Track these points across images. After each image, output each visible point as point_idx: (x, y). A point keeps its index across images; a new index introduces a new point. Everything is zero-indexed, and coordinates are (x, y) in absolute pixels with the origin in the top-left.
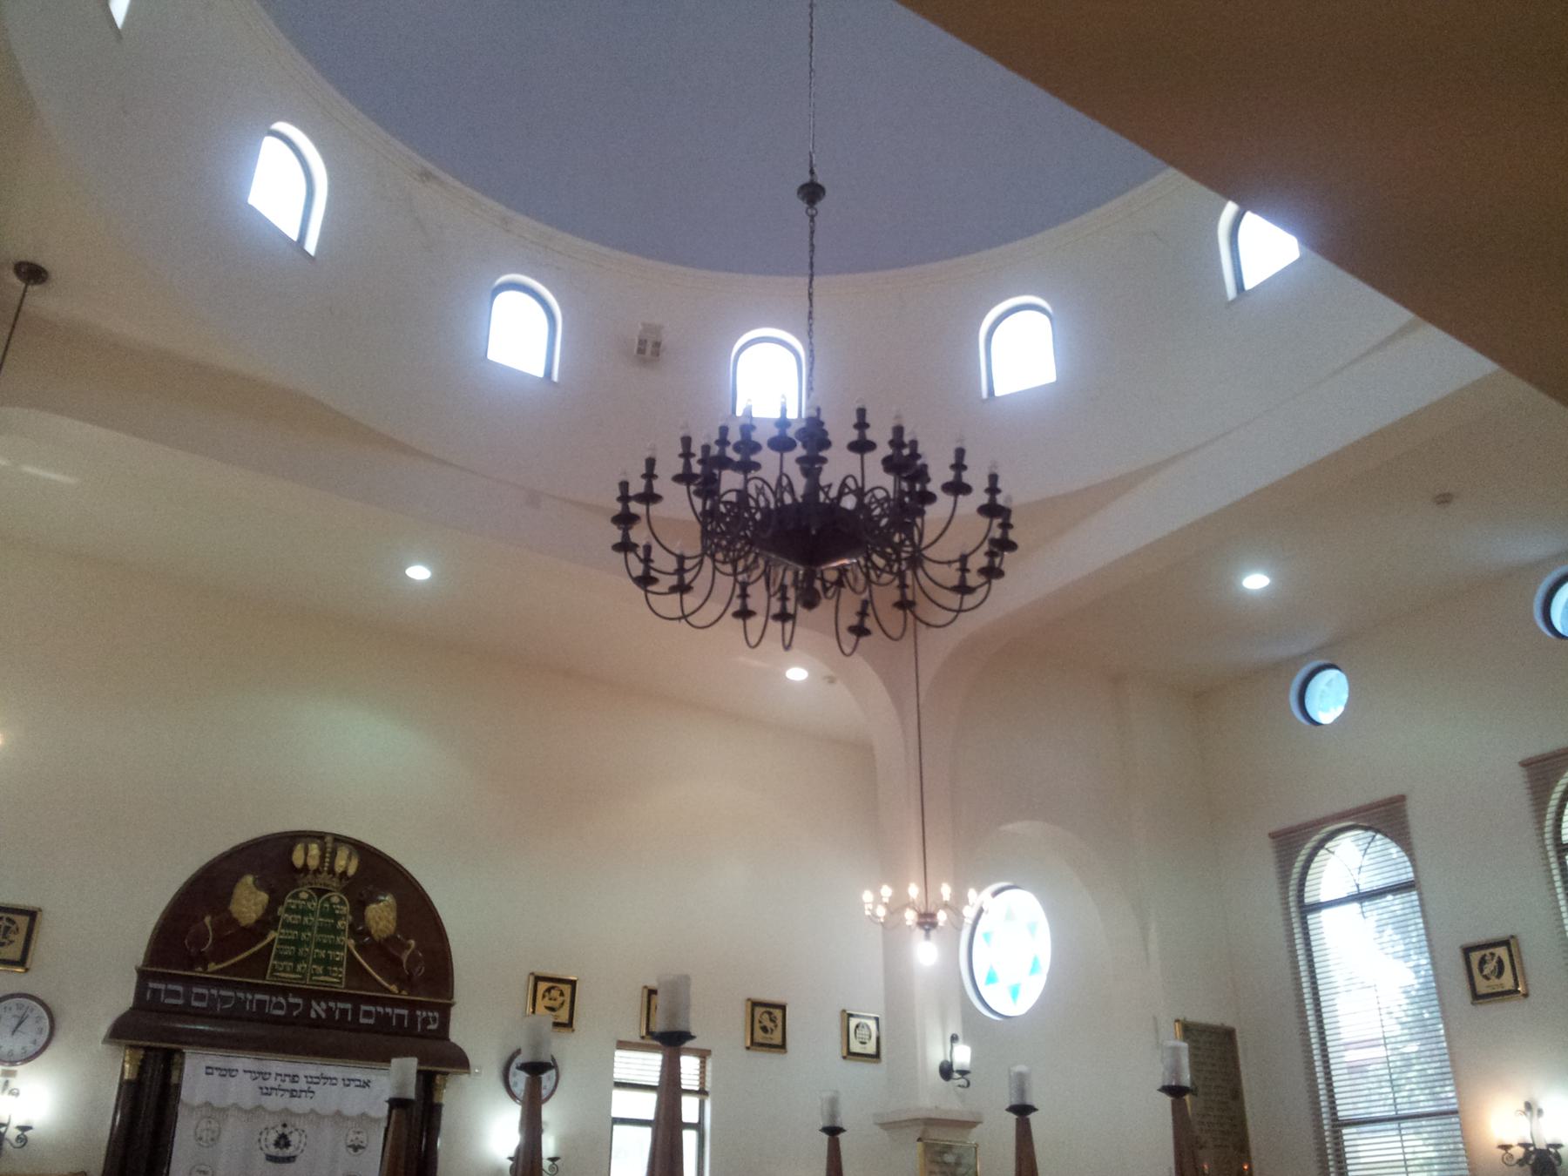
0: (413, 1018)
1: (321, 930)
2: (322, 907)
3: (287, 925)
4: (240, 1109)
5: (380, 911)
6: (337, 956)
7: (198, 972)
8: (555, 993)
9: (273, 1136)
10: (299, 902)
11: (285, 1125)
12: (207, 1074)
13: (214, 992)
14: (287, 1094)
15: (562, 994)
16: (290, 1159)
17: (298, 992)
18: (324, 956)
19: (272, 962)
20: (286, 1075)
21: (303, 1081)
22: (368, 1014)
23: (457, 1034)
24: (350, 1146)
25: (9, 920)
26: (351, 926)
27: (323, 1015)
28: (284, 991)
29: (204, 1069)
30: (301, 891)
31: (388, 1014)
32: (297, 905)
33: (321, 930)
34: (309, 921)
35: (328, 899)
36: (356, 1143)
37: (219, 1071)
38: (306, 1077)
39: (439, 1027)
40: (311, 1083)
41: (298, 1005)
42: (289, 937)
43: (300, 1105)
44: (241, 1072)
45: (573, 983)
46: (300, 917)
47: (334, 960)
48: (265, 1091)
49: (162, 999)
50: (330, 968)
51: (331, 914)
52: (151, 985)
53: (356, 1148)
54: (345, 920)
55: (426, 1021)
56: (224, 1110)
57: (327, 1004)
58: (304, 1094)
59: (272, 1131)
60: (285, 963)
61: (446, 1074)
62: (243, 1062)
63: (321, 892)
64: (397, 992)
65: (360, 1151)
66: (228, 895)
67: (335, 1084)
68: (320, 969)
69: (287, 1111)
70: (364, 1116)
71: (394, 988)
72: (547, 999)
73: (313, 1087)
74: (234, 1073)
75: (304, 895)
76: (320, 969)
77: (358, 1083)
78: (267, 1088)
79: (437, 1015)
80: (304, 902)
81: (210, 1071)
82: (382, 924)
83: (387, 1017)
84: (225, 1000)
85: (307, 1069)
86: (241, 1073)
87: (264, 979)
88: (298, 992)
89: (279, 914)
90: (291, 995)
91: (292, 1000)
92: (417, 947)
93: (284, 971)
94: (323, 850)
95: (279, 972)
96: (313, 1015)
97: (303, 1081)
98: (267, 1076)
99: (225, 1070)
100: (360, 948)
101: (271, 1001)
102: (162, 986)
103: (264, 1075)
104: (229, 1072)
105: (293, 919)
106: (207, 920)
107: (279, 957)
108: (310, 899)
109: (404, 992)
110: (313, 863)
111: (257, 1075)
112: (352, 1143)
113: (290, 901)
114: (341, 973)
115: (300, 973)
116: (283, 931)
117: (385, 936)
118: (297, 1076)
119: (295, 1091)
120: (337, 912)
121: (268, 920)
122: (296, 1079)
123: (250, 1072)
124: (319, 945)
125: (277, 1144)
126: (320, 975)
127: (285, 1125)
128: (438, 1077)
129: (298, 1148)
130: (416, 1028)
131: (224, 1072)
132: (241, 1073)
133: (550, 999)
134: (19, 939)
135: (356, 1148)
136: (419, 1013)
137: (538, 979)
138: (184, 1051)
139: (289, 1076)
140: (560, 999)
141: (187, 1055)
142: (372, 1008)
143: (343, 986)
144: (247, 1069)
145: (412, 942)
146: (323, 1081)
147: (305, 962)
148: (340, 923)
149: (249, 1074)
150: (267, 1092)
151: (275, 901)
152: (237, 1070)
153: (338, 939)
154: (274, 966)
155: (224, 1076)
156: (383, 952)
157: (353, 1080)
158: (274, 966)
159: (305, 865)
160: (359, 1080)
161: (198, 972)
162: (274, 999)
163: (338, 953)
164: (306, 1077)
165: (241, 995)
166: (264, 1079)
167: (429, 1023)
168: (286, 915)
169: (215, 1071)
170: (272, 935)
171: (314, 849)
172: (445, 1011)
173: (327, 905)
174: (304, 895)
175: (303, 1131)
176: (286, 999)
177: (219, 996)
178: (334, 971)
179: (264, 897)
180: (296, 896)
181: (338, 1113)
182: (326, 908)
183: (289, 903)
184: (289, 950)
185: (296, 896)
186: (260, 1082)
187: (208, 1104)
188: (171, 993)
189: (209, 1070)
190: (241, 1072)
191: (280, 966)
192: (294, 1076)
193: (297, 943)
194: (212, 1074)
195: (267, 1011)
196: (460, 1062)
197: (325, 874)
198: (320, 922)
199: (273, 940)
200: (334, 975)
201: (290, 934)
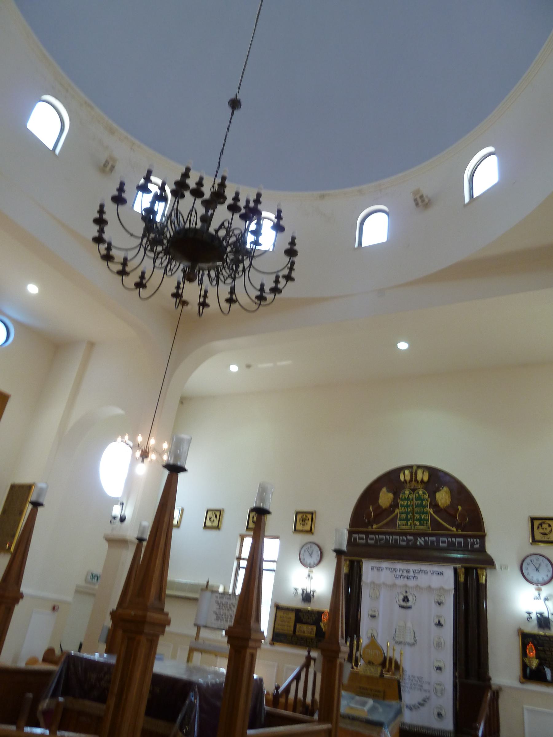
0: (466, 543)
1: (417, 506)
2: (415, 495)
3: (402, 506)
4: (385, 584)
8: (545, 526)
9: (401, 597)
13: (377, 536)
14: (406, 579)
16: (409, 608)
17: (411, 534)
22: (443, 542)
23: (491, 548)
26: (430, 503)
27: (423, 543)
28: (405, 534)
31: (454, 542)
33: (417, 506)
36: (439, 601)
41: (412, 540)
43: (411, 583)
51: (420, 498)
55: (473, 544)
62: (385, 564)
66: (378, 498)
68: (418, 523)
69: (406, 586)
75: (407, 492)
79: (478, 540)
82: (443, 501)
83: (453, 544)
84: (381, 540)
85: (413, 567)
88: (411, 534)
89: (398, 501)
92: (462, 509)
93: (403, 525)
96: (418, 543)
100: (434, 512)
103: (395, 570)
104: (380, 569)
106: (371, 508)
108: (410, 493)
110: (408, 478)
117: (446, 505)
121: (394, 505)
124: (417, 513)
125: (404, 600)
127: (406, 592)
132: (385, 570)
134: (309, 523)
135: (439, 604)
136: (469, 540)
137: (533, 520)
140: (549, 529)
141: (363, 562)
142: (445, 539)
145: (460, 508)
147: (412, 521)
150: (396, 577)
151: (396, 495)
153: (425, 510)
159: (405, 480)
161: (370, 529)
162: (401, 538)
165: (388, 537)
170: (397, 511)
171: (407, 472)
172: (483, 537)
173: (417, 495)
174: (407, 492)
179: (391, 495)
181: (429, 588)
184: (404, 516)
185: (404, 493)
187: (373, 583)
188: (361, 539)
193: (407, 513)
199: (397, 514)
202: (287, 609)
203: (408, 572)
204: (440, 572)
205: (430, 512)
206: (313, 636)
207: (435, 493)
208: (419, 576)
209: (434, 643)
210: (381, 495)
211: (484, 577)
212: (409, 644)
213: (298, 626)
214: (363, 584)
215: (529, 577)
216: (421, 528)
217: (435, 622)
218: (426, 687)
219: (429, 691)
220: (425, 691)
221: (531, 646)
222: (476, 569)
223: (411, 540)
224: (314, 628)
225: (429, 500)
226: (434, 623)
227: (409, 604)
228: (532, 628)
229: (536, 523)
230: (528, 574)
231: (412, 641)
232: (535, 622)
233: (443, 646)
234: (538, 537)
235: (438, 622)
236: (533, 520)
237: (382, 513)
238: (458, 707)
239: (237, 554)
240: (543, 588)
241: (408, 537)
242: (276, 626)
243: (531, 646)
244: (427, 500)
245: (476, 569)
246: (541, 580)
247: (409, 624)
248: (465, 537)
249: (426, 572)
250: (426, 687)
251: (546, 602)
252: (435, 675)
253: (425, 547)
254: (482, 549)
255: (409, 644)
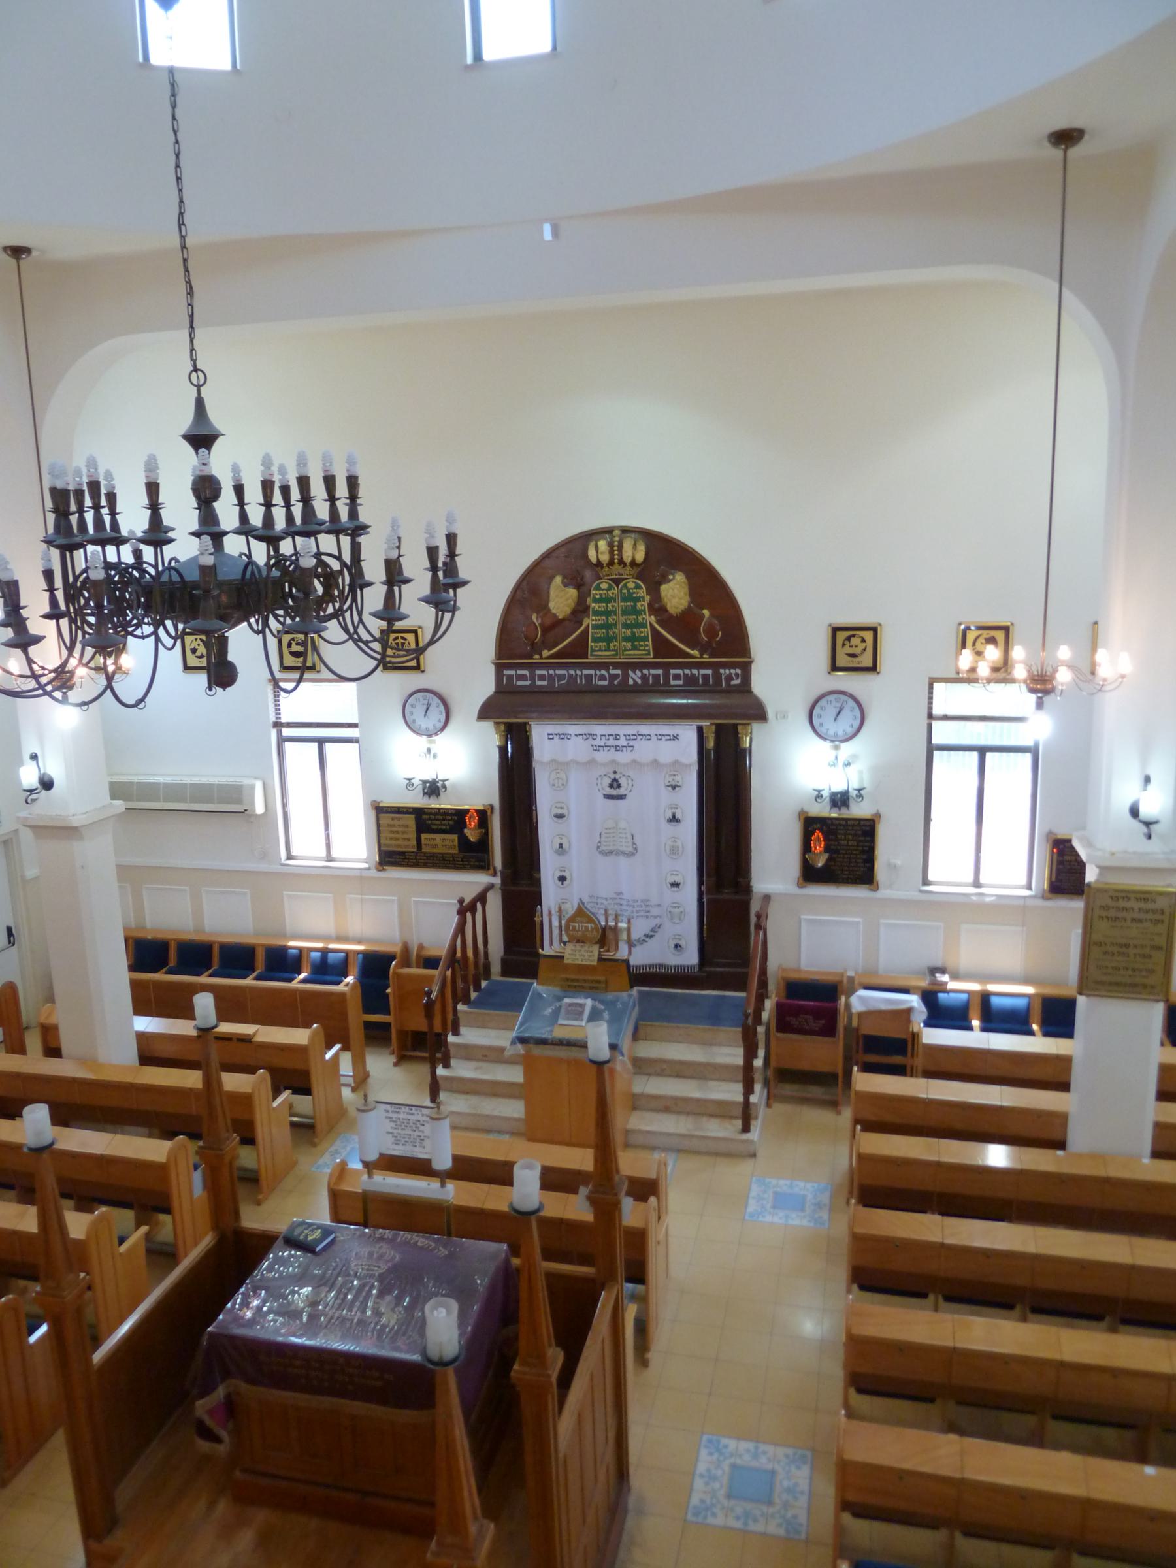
0: (717, 676)
1: (625, 612)
2: (621, 592)
3: (596, 613)
4: (577, 763)
5: (671, 591)
6: (641, 632)
7: (536, 659)
8: (854, 641)
9: (607, 781)
10: (601, 592)
11: (615, 772)
12: (549, 739)
13: (551, 672)
14: (613, 750)
15: (863, 640)
16: (622, 797)
17: (616, 665)
18: (630, 634)
19: (590, 644)
20: (609, 735)
21: (623, 738)
22: (677, 677)
23: (759, 686)
24: (668, 786)
25: (403, 638)
26: (650, 605)
27: (639, 681)
28: (605, 666)
29: (547, 736)
30: (601, 583)
32: (600, 594)
33: (625, 612)
34: (613, 606)
35: (625, 585)
36: (674, 783)
37: (558, 736)
38: (625, 735)
39: (742, 681)
40: (629, 740)
41: (619, 674)
42: (600, 622)
43: (623, 757)
44: (573, 735)
45: (874, 630)
46: (604, 604)
47: (639, 637)
48: (595, 748)
49: (515, 683)
50: (636, 643)
51: (629, 597)
52: (506, 672)
53: (674, 787)
54: (644, 601)
55: (729, 678)
56: (567, 764)
57: (641, 672)
58: (624, 749)
59: (605, 777)
60: (601, 644)
61: (748, 724)
63: (617, 582)
64: (699, 656)
65: (677, 789)
67: (649, 739)
69: (614, 762)
70: (676, 762)
71: (695, 653)
72: (847, 646)
73: (632, 743)
74: (569, 737)
75: (604, 586)
76: (629, 645)
77: (668, 738)
78: (596, 746)
79: (739, 671)
80: (605, 592)
81: (551, 737)
82: (675, 601)
84: (561, 677)
85: (625, 729)
86: (573, 736)
87: (587, 658)
88: (616, 665)
89: (588, 603)
90: (611, 667)
91: (613, 672)
92: (711, 615)
93: (600, 650)
94: (611, 545)
95: (596, 651)
96: (631, 682)
97: (623, 738)
98: (595, 737)
99: (563, 734)
100: (658, 622)
101: (596, 675)
102: (512, 672)
104: (564, 736)
105: (599, 607)
107: (595, 640)
109: (705, 656)
110: (605, 558)
111: (588, 736)
112: (669, 784)
113: (594, 592)
114: (647, 645)
115: (613, 651)
116: (594, 618)
118: (619, 735)
119: (619, 746)
120: (634, 595)
121: (580, 610)
122: (618, 737)
123: (580, 735)
124: (626, 626)
125: (611, 786)
126: (630, 650)
127: (615, 772)
128: (740, 728)
129: (627, 789)
130: (722, 685)
131: (562, 736)
133: (851, 647)
135: (674, 787)
136: (722, 671)
137: (835, 630)
138: (530, 723)
139: (612, 735)
141: (532, 726)
142: (679, 671)
143: (652, 656)
144: (577, 733)
145: (706, 612)
146: (639, 737)
148: (639, 604)
149: (581, 737)
150: (596, 748)
152: (570, 735)
154: (592, 646)
155: (562, 738)
156: (684, 624)
157: (664, 735)
158: (592, 646)
159: (599, 564)
160: (670, 735)
161: (536, 659)
162: (598, 672)
163: (642, 630)
164: (625, 735)
165: (572, 672)
166: (594, 739)
167: (734, 680)
168: (594, 604)
169: (555, 736)
170: (586, 622)
171: (603, 544)
172: (746, 668)
175: (629, 776)
176: (608, 670)
177: (555, 674)
178: (642, 646)
179: (572, 592)
180: (598, 588)
181: (655, 763)
182: (625, 593)
183: (593, 594)
185: (598, 588)
186: (591, 741)
187: (553, 761)
188: (521, 678)
189: (551, 736)
190: (573, 735)
191: (596, 647)
192: (616, 735)
193: (607, 626)
194: (553, 739)
195: (594, 683)
196: (759, 713)
197: (616, 566)
198: (622, 606)
200: (643, 648)
201: (599, 620)
202: (399, 810)
203: (617, 737)
204: (673, 736)
205: (650, 622)
206: (455, 851)
207: (659, 583)
208: (639, 744)
209: (665, 850)
210: (553, 593)
211: (748, 738)
212: (623, 853)
213: (424, 836)
214: (534, 765)
215: (821, 730)
216: (635, 655)
217: (667, 817)
218: (655, 911)
219: (660, 917)
220: (655, 917)
221: (818, 834)
222: (735, 726)
223: (617, 676)
224: (455, 837)
225: (647, 598)
226: (665, 818)
227: (622, 791)
228: (823, 810)
229: (841, 636)
230: (821, 725)
231: (630, 849)
232: (827, 802)
233: (680, 852)
234: (842, 661)
235: (671, 817)
236: (835, 630)
237: (554, 626)
238: (705, 935)
239: (273, 718)
240: (843, 745)
241: (613, 672)
242: (382, 842)
243: (818, 834)
244: (644, 601)
245: (735, 726)
246: (840, 733)
247: (622, 824)
248: (715, 666)
249: (648, 737)
250: (655, 911)
251: (848, 769)
252: (670, 895)
253: (645, 688)
254: (745, 687)
255: (623, 853)
